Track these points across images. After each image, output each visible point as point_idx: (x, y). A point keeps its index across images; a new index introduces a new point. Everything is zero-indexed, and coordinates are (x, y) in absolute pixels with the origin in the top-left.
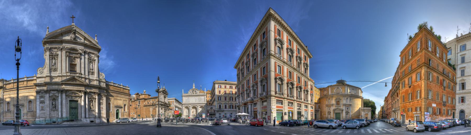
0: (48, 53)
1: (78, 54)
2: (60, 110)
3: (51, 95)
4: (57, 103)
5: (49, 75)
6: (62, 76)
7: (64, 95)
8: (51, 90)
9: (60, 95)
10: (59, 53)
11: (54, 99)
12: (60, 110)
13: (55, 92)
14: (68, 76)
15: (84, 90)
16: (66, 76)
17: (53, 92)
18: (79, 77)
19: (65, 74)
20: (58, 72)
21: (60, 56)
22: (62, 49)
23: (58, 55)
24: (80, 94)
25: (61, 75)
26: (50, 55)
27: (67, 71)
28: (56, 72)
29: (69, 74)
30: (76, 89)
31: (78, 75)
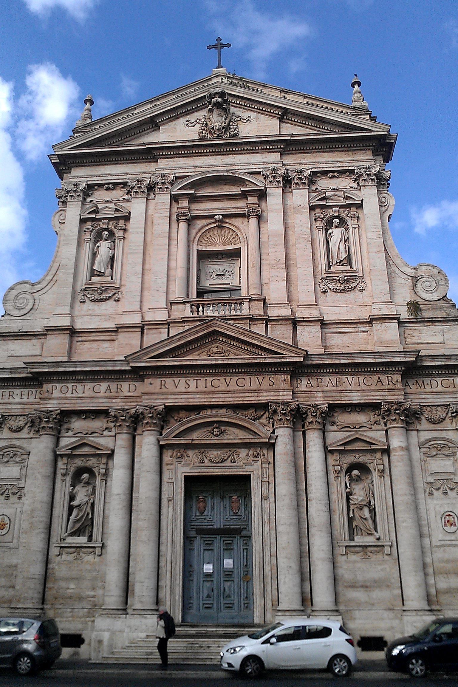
0: (74, 211)
1: (244, 195)
2: (115, 545)
3: (66, 441)
4: (99, 498)
5: (65, 322)
6: (142, 328)
7: (147, 443)
8: (66, 415)
9: (123, 440)
10: (137, 207)
11: (85, 471)
12: (115, 545)
13: (97, 424)
14: (184, 321)
15: (285, 396)
16: (167, 324)
17: (77, 424)
18: (252, 319)
19: (162, 316)
20: (122, 306)
21: (136, 223)
22: (151, 188)
23: (127, 218)
24: (263, 429)
25: (136, 320)
26: (83, 221)
27: (177, 293)
28: (109, 307)
29: (186, 311)
30: (231, 400)
31: (245, 309)
